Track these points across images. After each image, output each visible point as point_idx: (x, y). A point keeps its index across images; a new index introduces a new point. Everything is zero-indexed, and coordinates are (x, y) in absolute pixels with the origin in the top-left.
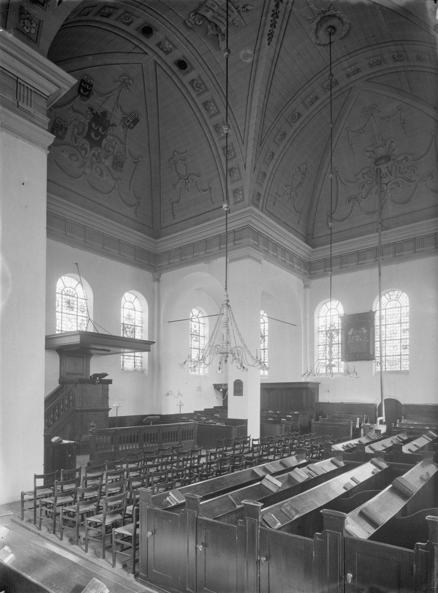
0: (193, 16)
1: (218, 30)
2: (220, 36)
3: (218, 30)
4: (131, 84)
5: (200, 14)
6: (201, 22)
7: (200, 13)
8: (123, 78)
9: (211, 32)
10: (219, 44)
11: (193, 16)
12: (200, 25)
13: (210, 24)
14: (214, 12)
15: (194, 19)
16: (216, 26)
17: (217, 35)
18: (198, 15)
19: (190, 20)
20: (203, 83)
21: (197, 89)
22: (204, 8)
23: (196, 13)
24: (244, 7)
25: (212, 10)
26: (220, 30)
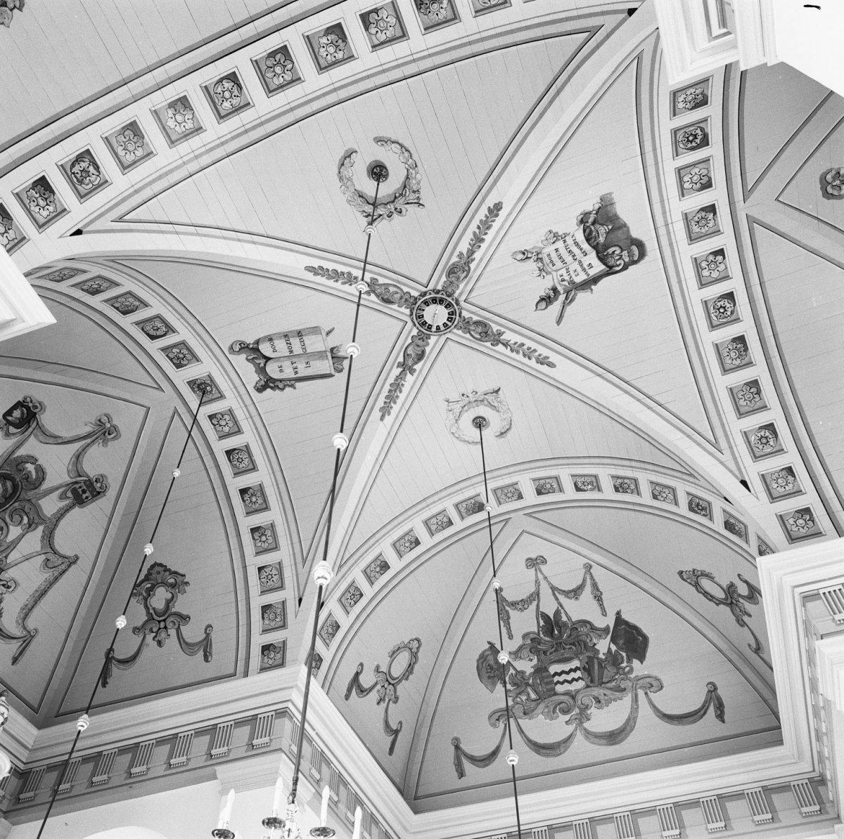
0: (620, 265)
1: (588, 231)
2: (591, 220)
3: (588, 231)
4: (834, 172)
5: (605, 264)
6: (610, 251)
7: (603, 267)
8: (836, 193)
9: (602, 230)
10: (600, 208)
11: (620, 265)
12: (615, 246)
13: (598, 243)
14: (580, 262)
15: (618, 259)
16: (588, 240)
17: (593, 224)
18: (611, 262)
19: (627, 260)
20: (676, 143)
21: (699, 132)
22: (592, 272)
23: (611, 267)
24: (527, 258)
25: (582, 266)
26: (584, 231)
